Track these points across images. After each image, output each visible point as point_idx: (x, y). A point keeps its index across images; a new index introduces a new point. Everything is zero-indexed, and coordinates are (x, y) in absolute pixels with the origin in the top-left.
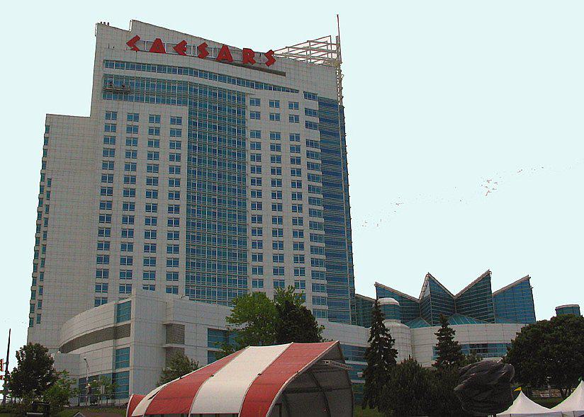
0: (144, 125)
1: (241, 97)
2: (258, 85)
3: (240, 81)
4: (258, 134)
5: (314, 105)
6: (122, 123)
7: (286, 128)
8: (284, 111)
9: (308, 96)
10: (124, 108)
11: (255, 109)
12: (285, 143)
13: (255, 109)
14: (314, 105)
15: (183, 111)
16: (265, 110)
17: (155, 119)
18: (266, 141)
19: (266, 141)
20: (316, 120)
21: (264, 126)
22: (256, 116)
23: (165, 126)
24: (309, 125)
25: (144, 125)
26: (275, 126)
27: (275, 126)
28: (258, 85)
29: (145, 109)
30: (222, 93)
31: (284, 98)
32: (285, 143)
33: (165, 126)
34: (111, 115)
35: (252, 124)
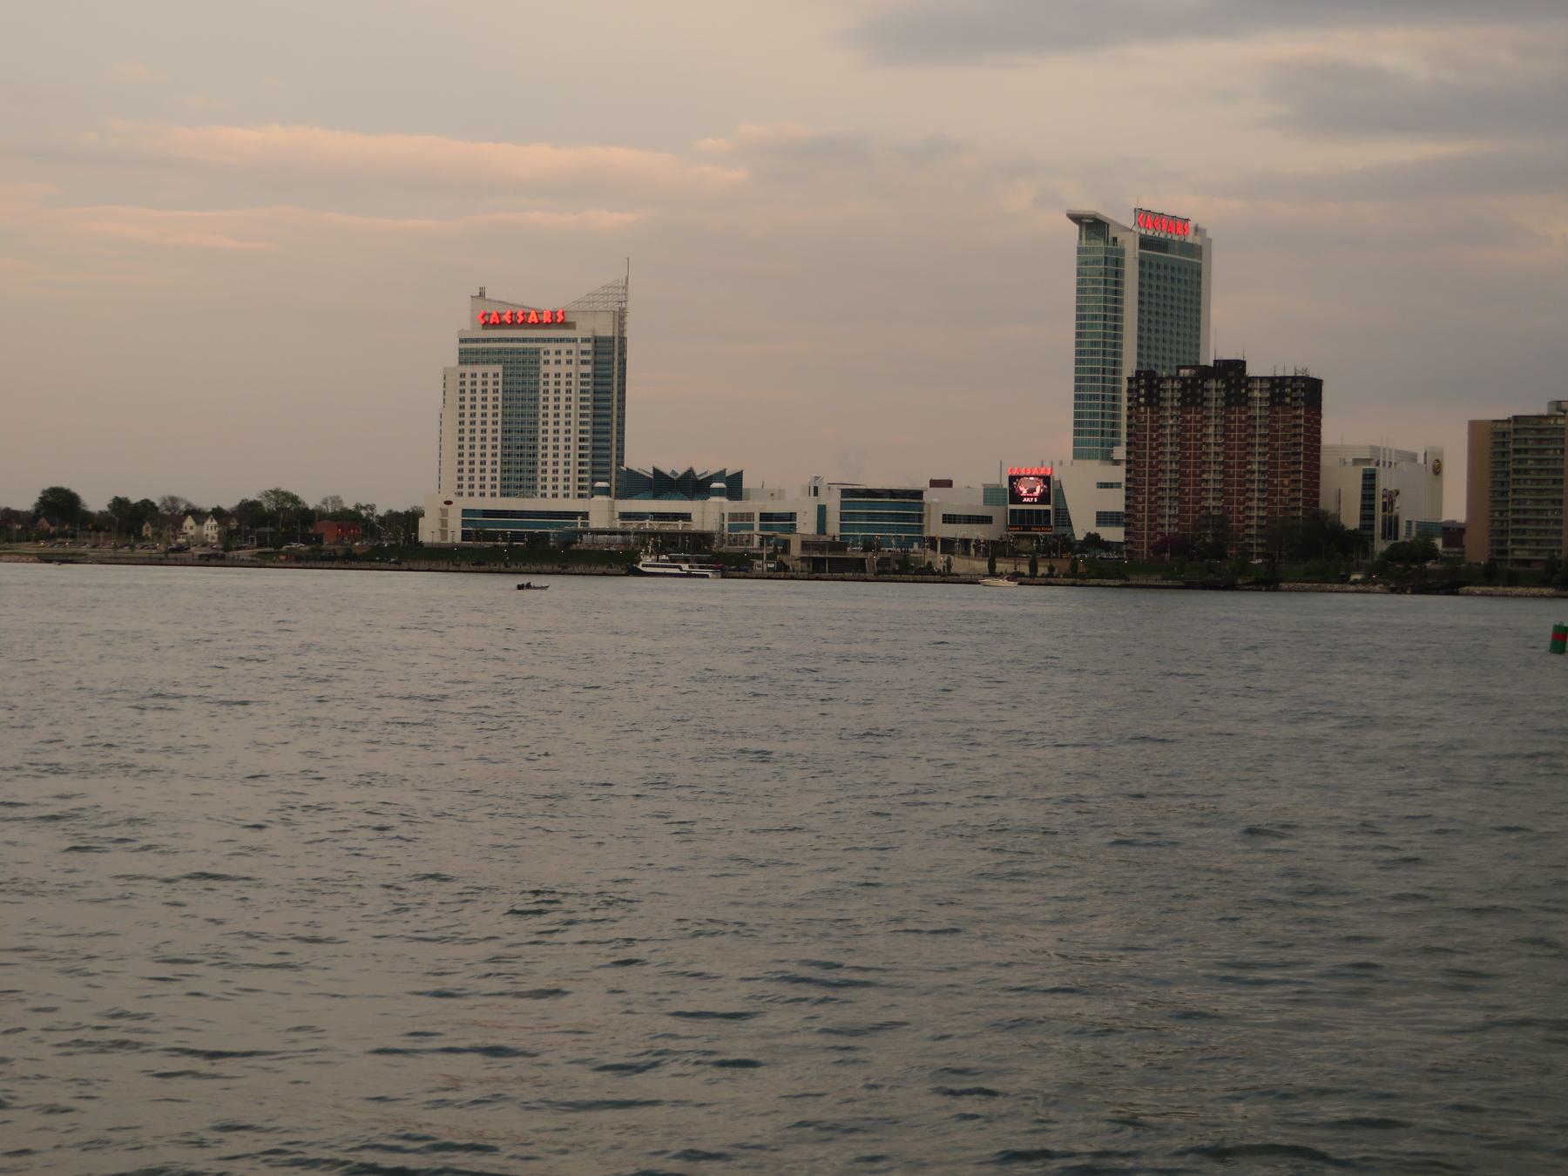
0: (479, 379)
1: (537, 352)
2: (549, 340)
3: (537, 340)
4: (547, 375)
5: (588, 347)
6: (468, 380)
7: (563, 369)
8: (564, 357)
9: (585, 340)
10: (468, 369)
11: (545, 358)
12: (563, 379)
13: (545, 358)
14: (588, 347)
15: (499, 369)
16: (552, 358)
17: (485, 375)
18: (552, 379)
19: (552, 379)
20: (588, 358)
21: (551, 369)
22: (547, 362)
23: (490, 379)
24: (584, 362)
25: (479, 379)
26: (558, 369)
27: (558, 369)
28: (549, 340)
29: (480, 369)
30: (524, 351)
31: (564, 347)
32: (563, 379)
33: (490, 379)
34: (462, 375)
35: (544, 369)
